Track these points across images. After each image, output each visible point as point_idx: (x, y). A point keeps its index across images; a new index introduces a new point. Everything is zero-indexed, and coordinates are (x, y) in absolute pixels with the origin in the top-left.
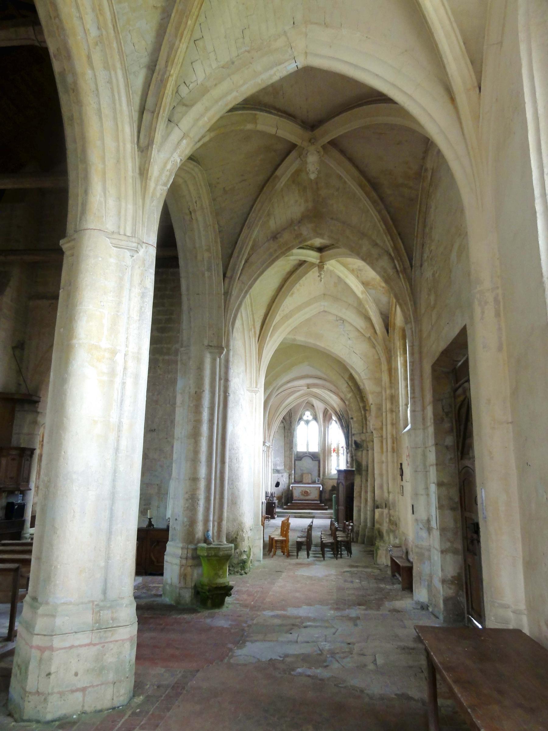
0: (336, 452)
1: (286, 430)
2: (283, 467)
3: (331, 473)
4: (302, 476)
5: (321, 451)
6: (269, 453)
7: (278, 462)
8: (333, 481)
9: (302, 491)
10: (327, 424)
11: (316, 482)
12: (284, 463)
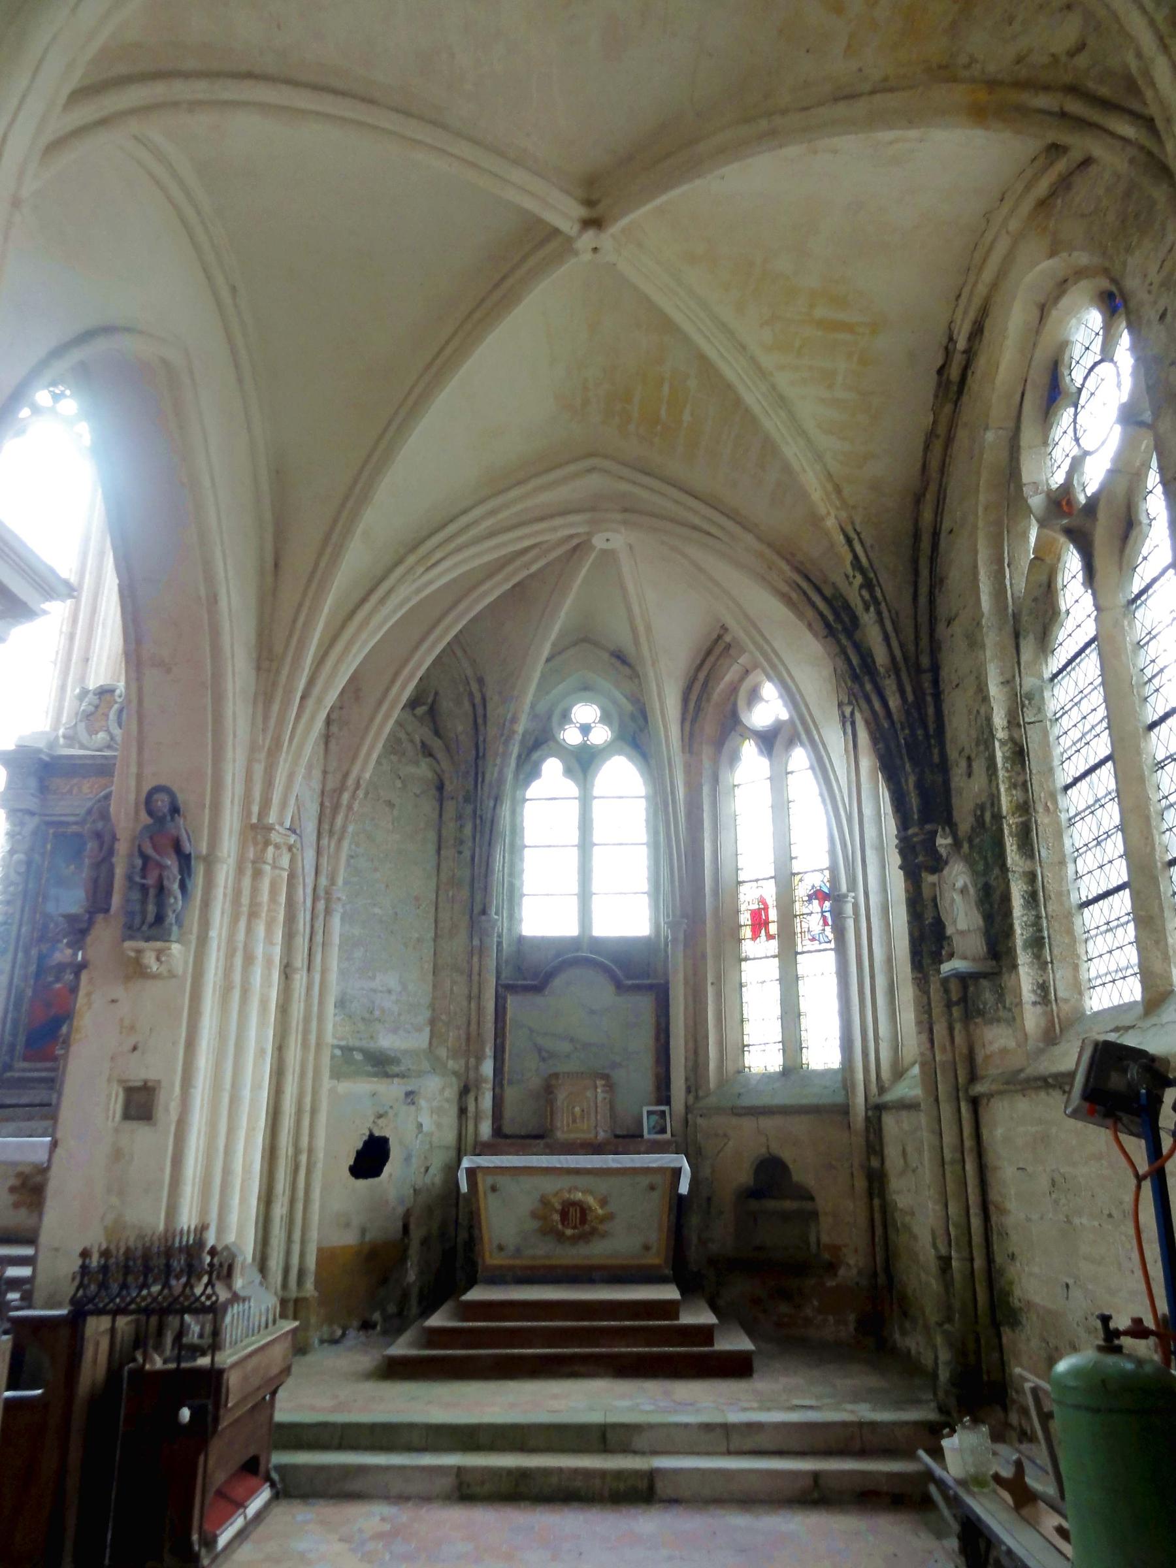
0: (773, 929)
1: (450, 807)
2: (420, 1040)
3: (741, 1070)
4: (548, 1089)
5: (673, 926)
6: (255, 891)
7: (388, 1003)
8: (766, 1123)
9: (545, 1202)
10: (707, 763)
11: (642, 1136)
12: (432, 1007)
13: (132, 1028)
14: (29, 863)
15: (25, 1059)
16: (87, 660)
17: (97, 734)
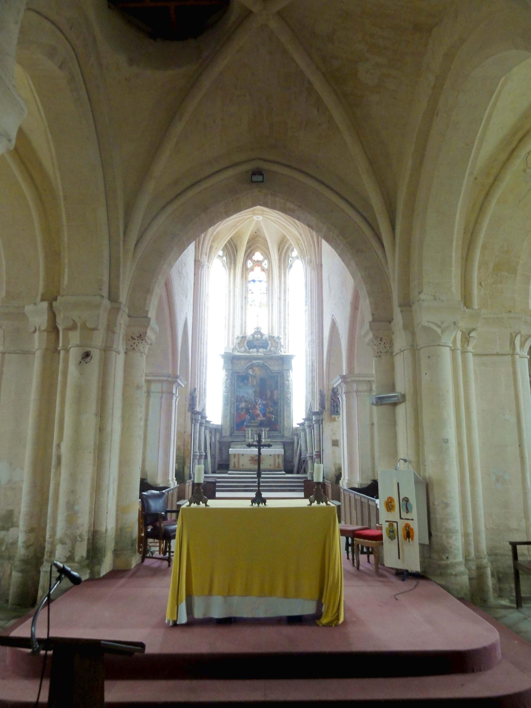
13: (333, 430)
14: (231, 382)
15: (237, 430)
16: (234, 327)
17: (242, 348)
